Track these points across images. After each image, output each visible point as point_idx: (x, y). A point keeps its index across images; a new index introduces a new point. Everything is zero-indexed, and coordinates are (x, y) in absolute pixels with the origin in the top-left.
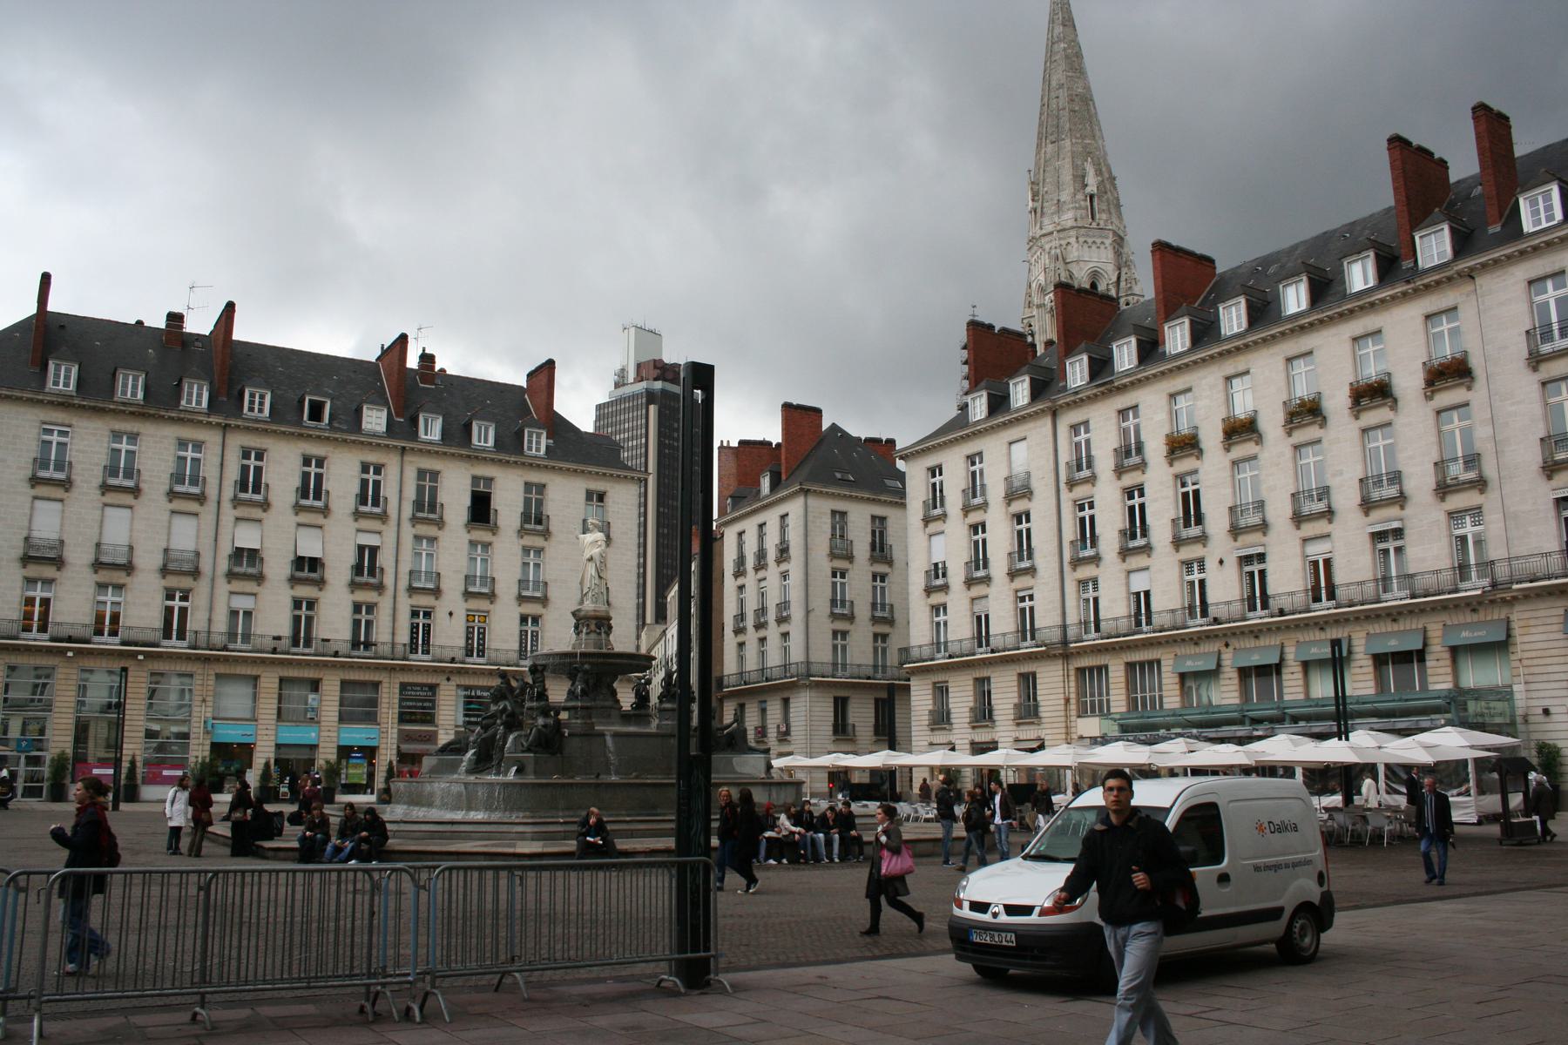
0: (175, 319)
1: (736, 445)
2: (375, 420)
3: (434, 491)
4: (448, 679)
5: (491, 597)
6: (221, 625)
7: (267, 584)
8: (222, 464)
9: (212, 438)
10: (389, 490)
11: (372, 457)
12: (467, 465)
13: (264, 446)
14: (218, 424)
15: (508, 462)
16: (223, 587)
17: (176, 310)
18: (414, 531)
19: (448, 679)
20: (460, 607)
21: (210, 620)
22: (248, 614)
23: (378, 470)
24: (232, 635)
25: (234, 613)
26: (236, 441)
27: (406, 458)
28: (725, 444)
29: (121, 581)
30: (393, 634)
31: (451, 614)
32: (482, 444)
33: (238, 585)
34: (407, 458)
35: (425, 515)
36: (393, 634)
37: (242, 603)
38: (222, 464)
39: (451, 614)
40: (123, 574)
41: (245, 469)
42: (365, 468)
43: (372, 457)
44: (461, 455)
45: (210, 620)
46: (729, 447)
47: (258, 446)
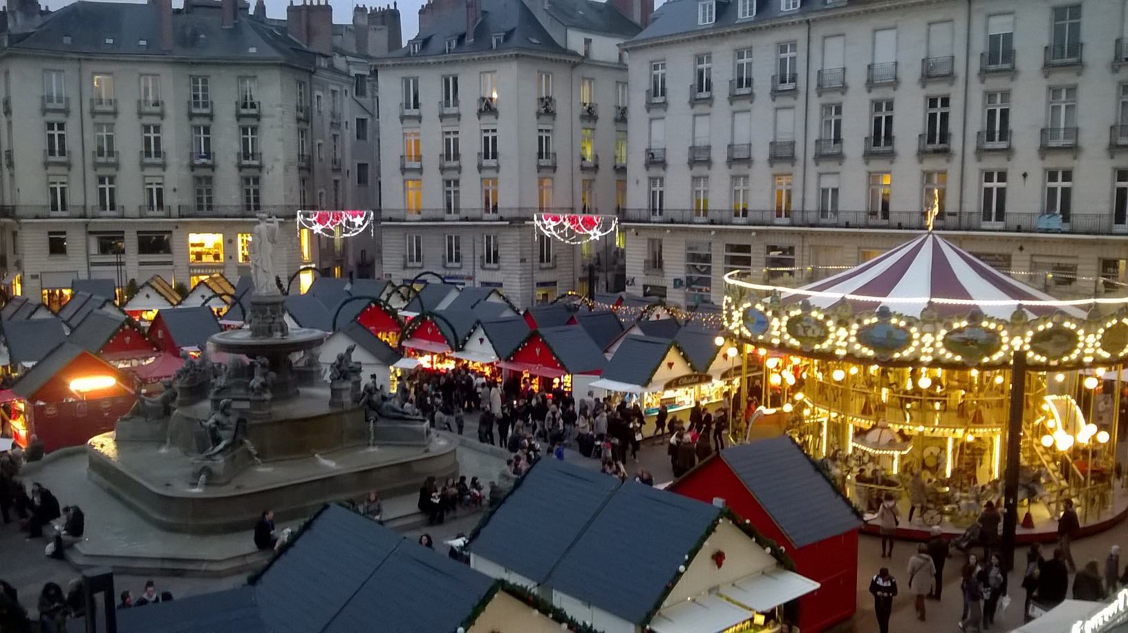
3: (1075, 29)
4: (1021, 249)
5: (1074, 149)
6: (812, 204)
7: (847, 163)
14: (800, 22)
16: (813, 170)
18: (984, 87)
19: (1021, 249)
20: (1037, 169)
21: (804, 200)
22: (835, 191)
24: (823, 212)
25: (825, 191)
29: (746, 173)
30: (961, 202)
31: (1025, 175)
33: (826, 166)
35: (1001, 66)
36: (961, 202)
37: (829, 183)
39: (1025, 175)
40: (745, 167)
45: (804, 200)
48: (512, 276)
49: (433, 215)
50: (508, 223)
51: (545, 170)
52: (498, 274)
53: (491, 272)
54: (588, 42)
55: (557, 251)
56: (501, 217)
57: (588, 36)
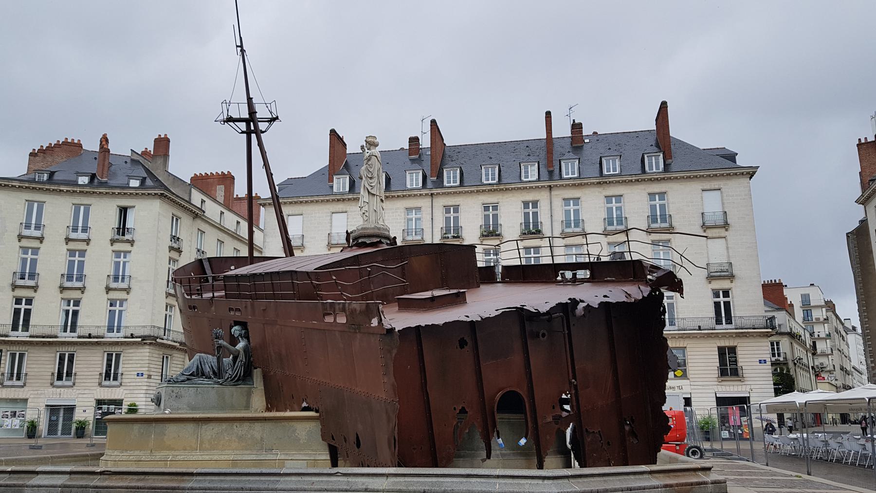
0: (414, 141)
1: (873, 139)
2: (532, 173)
8: (432, 219)
9: (425, 203)
10: (544, 218)
11: (530, 197)
12: (600, 189)
13: (457, 204)
14: (426, 195)
15: (631, 181)
17: (414, 136)
23: (535, 204)
26: (440, 202)
27: (552, 193)
28: (863, 141)
32: (612, 173)
34: (554, 193)
38: (432, 219)
41: (448, 220)
42: (526, 204)
43: (530, 197)
44: (593, 183)
46: (867, 143)
47: (454, 204)
48: (136, 392)
49: (48, 332)
50: (140, 340)
51: (171, 297)
52: (121, 390)
53: (110, 389)
54: (203, 201)
55: (173, 372)
56: (132, 335)
57: (205, 198)
